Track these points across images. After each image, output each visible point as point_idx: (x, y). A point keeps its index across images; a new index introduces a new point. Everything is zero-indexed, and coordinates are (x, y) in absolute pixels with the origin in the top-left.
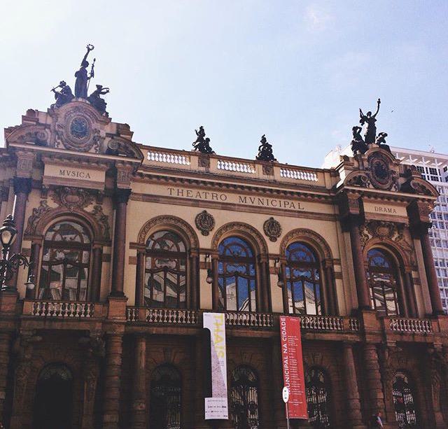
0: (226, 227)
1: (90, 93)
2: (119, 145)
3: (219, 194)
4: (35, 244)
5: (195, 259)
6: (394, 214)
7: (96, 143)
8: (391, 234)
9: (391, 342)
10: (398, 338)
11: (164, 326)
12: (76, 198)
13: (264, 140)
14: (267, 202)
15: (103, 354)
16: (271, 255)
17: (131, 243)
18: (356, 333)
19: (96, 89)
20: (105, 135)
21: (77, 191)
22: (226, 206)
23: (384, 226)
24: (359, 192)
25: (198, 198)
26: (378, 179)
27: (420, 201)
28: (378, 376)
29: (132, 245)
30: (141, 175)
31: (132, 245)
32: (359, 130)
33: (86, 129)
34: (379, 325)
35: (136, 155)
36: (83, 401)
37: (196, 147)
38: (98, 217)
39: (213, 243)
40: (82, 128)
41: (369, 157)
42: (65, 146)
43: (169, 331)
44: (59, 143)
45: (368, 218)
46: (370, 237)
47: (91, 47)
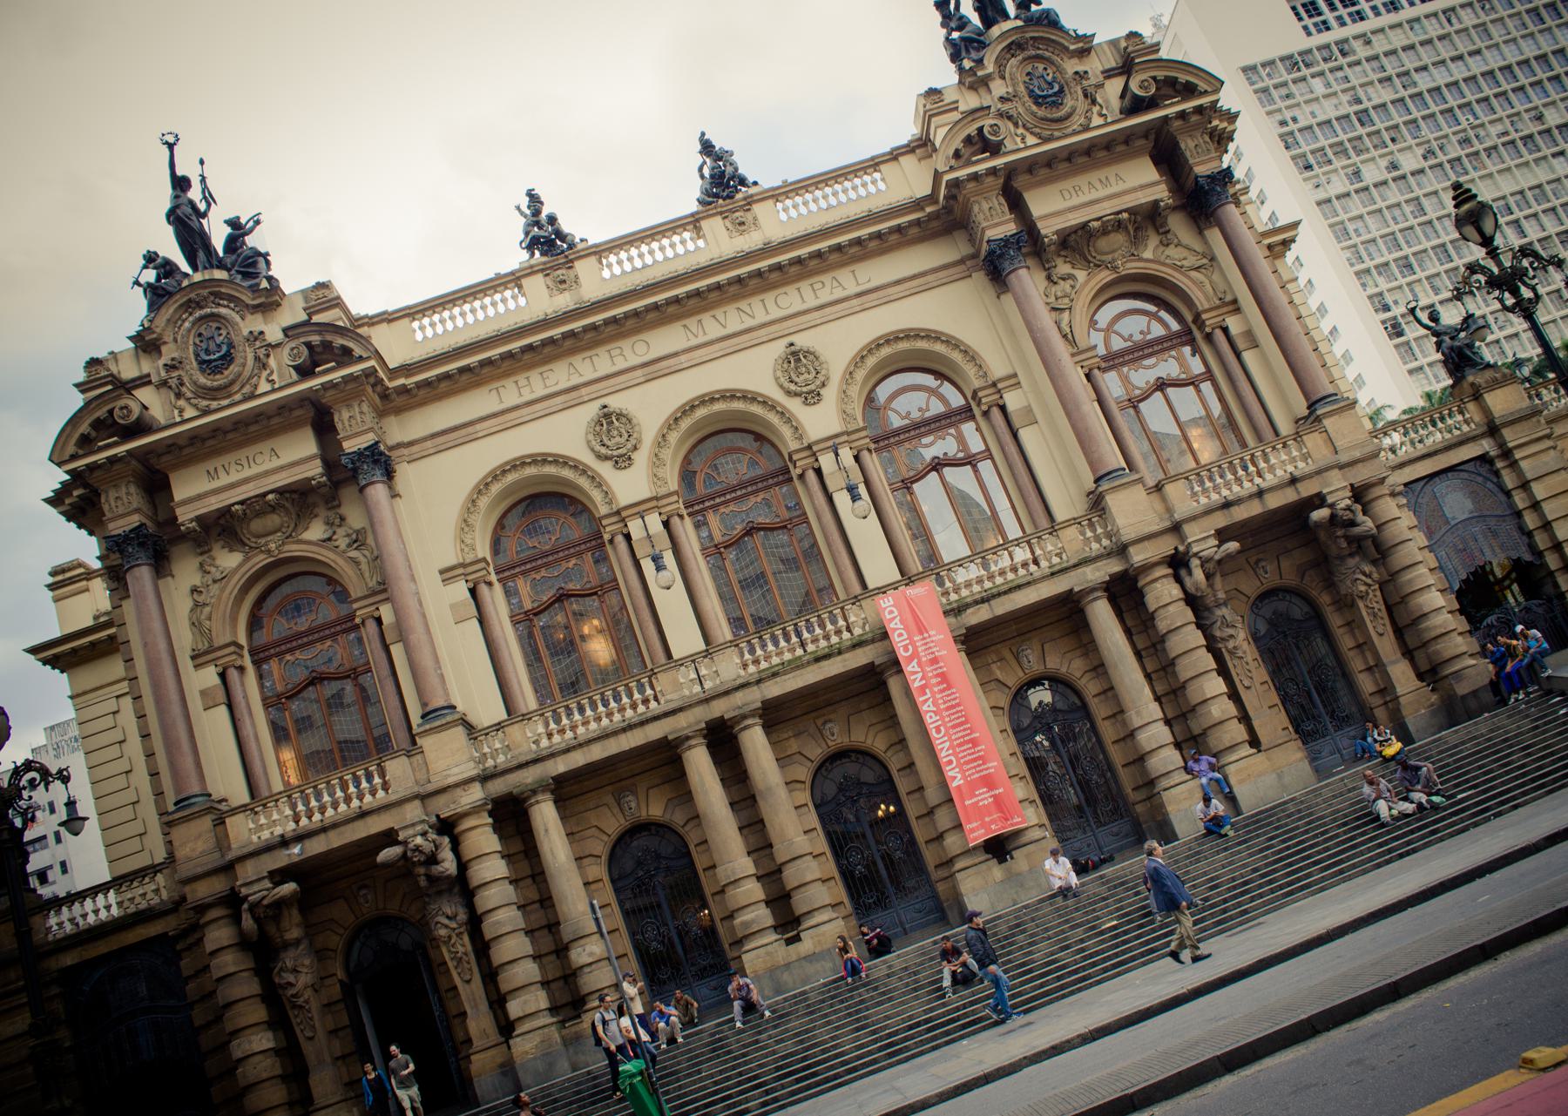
1: (218, 243)
2: (309, 345)
4: (225, 669)
5: (620, 539)
7: (265, 366)
9: (1201, 540)
10: (1220, 520)
11: (580, 745)
12: (274, 520)
15: (448, 864)
16: (818, 442)
17: (441, 572)
18: (1109, 554)
19: (228, 230)
20: (280, 336)
21: (257, 506)
22: (654, 369)
23: (1104, 231)
24: (993, 171)
26: (1041, 113)
27: (1178, 123)
28: (1196, 638)
29: (448, 575)
30: (403, 390)
31: (448, 575)
33: (231, 345)
34: (1159, 506)
35: (358, 351)
36: (455, 988)
37: (530, 248)
38: (342, 543)
40: (219, 346)
41: (1000, 64)
42: (195, 406)
43: (597, 753)
44: (181, 411)
45: (1048, 230)
46: (1081, 275)
47: (171, 139)
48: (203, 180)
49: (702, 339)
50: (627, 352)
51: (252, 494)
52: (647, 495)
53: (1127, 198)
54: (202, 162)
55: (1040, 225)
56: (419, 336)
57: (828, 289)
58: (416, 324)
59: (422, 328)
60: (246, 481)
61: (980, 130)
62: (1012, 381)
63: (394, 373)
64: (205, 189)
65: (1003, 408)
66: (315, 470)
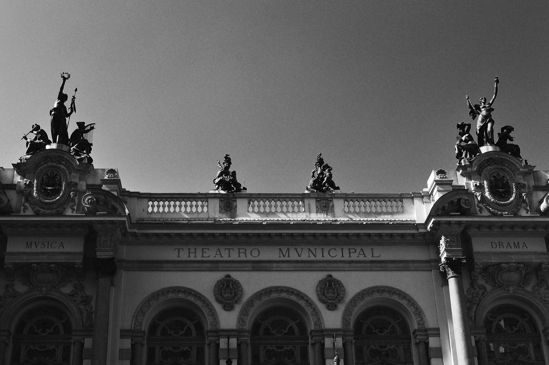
0: (259, 295)
3: (249, 249)
6: (525, 249)
8: (524, 280)
13: (320, 162)
14: (321, 254)
20: (85, 188)
22: (259, 266)
23: (509, 270)
25: (218, 258)
29: (124, 334)
30: (135, 235)
31: (124, 334)
32: (467, 127)
39: (241, 320)
45: (479, 261)
46: (489, 288)
47: (66, 76)
48: (74, 98)
49: (286, 258)
50: (248, 253)
51: (45, 261)
52: (235, 328)
53: (526, 257)
54: (76, 90)
55: (475, 257)
56: (150, 210)
57: (357, 253)
58: (150, 203)
59: (153, 206)
60: (43, 253)
61: (459, 200)
62: (435, 332)
63: (132, 225)
64: (73, 103)
65: (427, 344)
66: (79, 260)
